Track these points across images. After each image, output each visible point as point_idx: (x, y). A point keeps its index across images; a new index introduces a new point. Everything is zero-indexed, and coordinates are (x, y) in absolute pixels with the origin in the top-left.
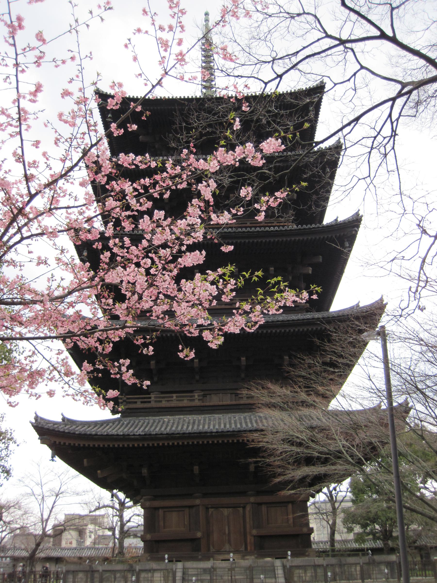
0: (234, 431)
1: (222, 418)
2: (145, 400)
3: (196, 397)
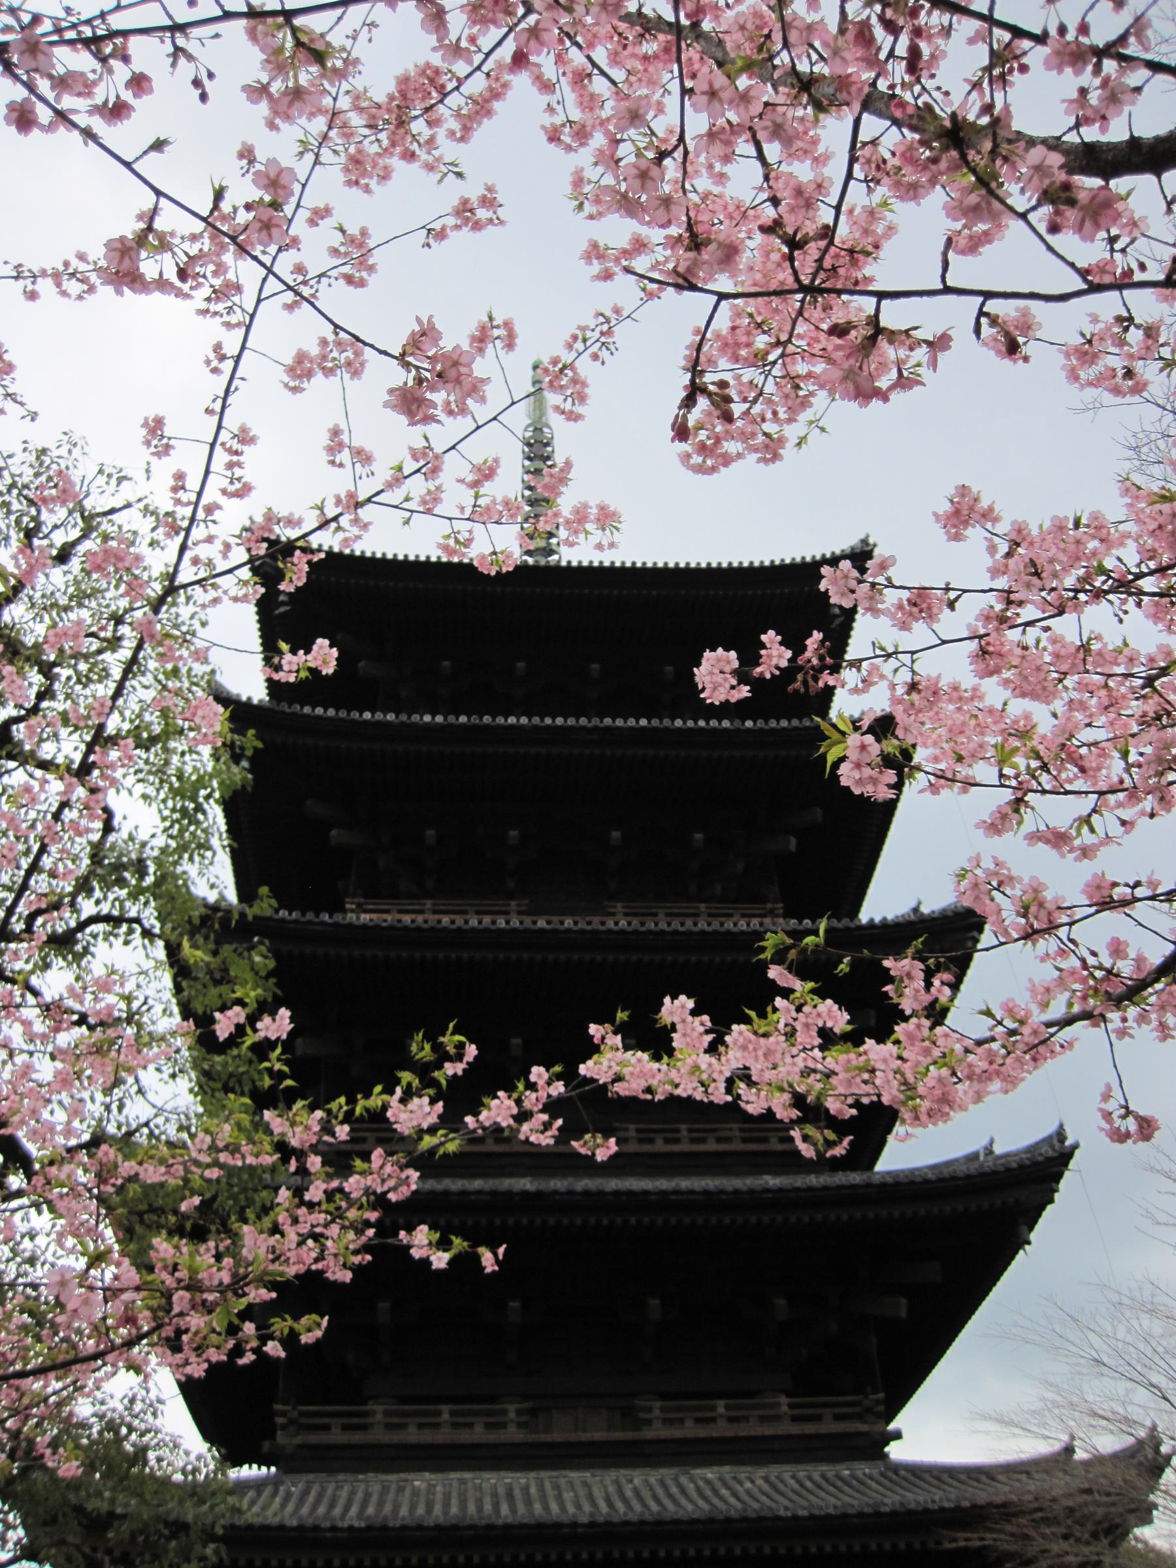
0: (642, 1523)
1: (590, 1480)
2: (356, 1420)
3: (512, 1415)
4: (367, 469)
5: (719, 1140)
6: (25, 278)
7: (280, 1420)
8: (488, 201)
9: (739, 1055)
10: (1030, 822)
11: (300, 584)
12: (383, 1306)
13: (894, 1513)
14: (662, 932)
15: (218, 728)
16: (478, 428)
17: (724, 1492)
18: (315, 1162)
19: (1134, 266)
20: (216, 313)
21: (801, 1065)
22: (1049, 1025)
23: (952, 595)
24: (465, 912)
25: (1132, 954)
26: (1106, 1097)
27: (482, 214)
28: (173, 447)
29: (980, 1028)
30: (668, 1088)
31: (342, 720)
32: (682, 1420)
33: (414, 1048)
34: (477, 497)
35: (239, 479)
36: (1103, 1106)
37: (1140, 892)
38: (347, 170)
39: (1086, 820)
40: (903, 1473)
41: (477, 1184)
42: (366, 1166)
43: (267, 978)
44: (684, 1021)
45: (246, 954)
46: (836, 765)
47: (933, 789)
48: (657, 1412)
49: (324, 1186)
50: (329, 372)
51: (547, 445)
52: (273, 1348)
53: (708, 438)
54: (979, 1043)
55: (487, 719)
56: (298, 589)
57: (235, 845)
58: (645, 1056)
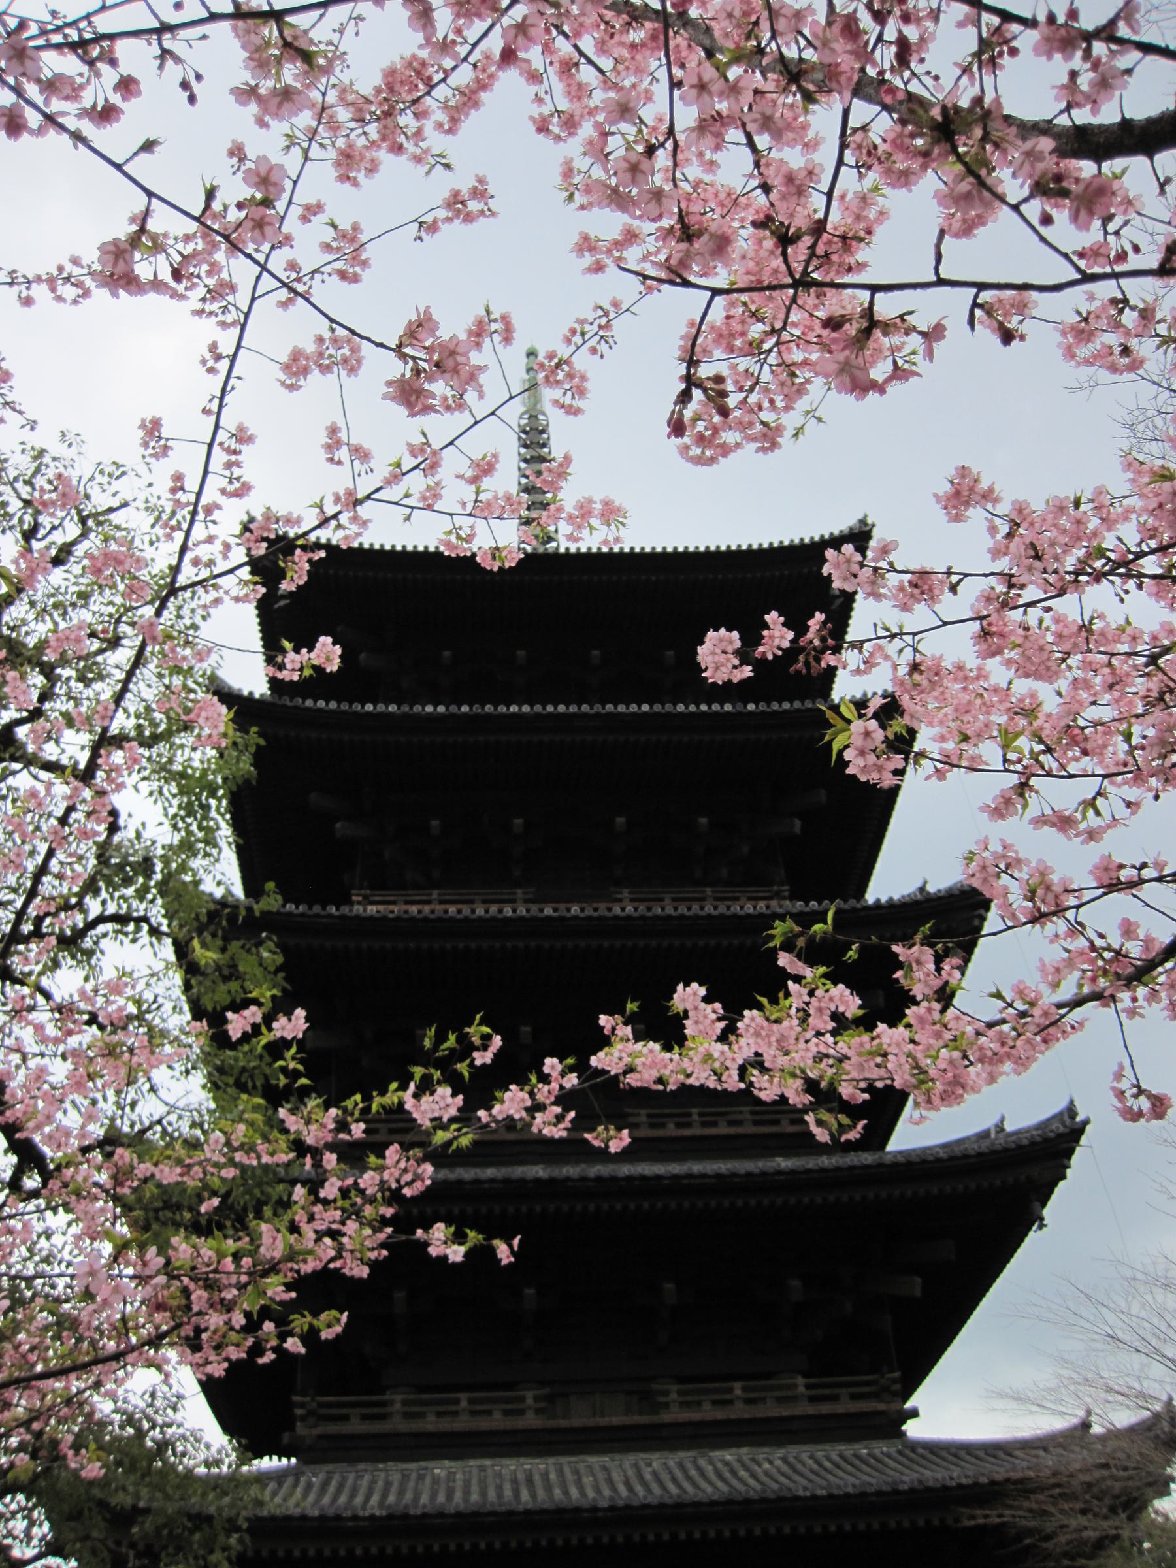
0: (662, 1506)
1: (609, 1465)
2: (376, 1410)
3: (530, 1401)
4: (366, 466)
5: (731, 1123)
6: (19, 284)
7: (299, 1412)
8: (479, 193)
9: (751, 1041)
10: (1036, 805)
11: (301, 583)
12: (399, 1295)
13: (912, 1491)
14: (670, 917)
15: (222, 729)
16: (476, 423)
17: (742, 1473)
18: (330, 1160)
19: (1128, 248)
20: (211, 313)
21: (814, 1049)
22: (1059, 1006)
23: (954, 579)
24: (472, 902)
25: (1142, 934)
26: (1119, 1076)
27: (474, 205)
28: (171, 448)
29: (991, 1010)
30: (681, 1077)
31: (344, 712)
32: (699, 1403)
33: (427, 1043)
34: (477, 493)
35: (238, 479)
36: (1115, 1084)
37: (1147, 873)
38: (338, 164)
39: (1091, 803)
40: (920, 1451)
41: (490, 1172)
42: (380, 1161)
43: (276, 972)
44: (696, 1008)
45: (254, 950)
46: (840, 753)
47: (940, 774)
48: (674, 1396)
49: (339, 1184)
50: (325, 370)
51: (543, 432)
52: (293, 1345)
53: (706, 429)
54: (990, 1025)
55: (489, 708)
56: (299, 587)
57: (241, 842)
58: (656, 1047)
